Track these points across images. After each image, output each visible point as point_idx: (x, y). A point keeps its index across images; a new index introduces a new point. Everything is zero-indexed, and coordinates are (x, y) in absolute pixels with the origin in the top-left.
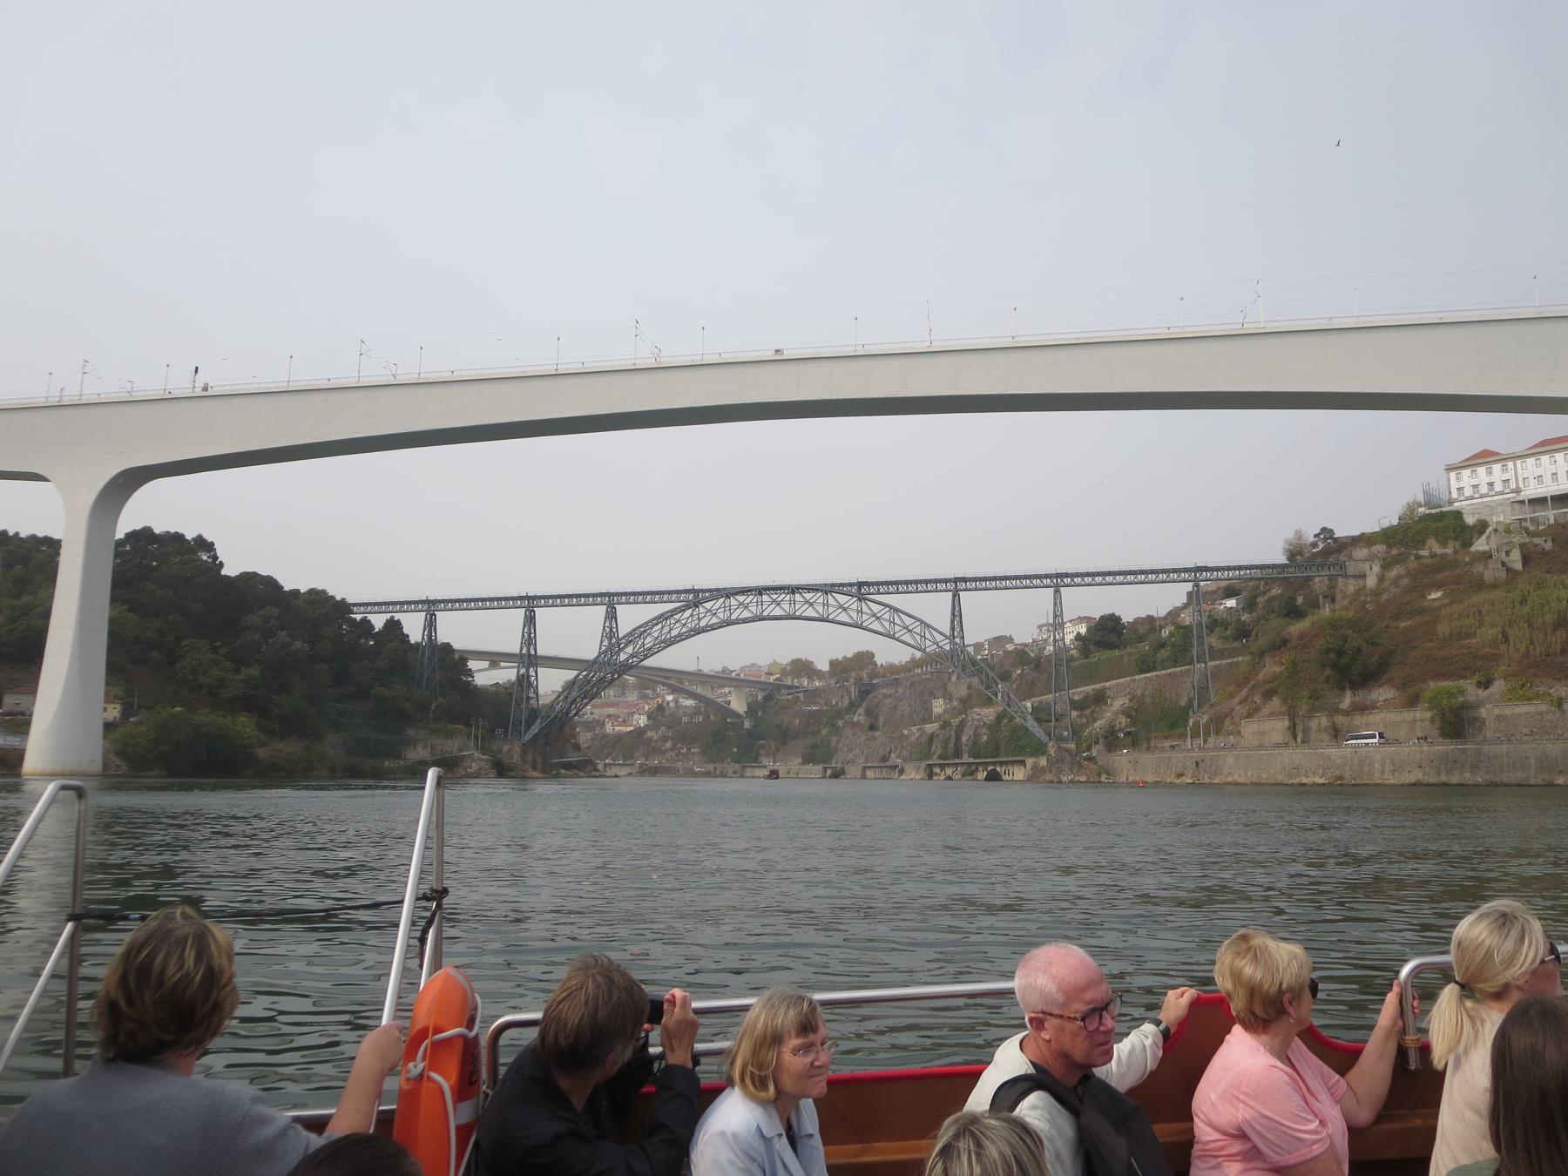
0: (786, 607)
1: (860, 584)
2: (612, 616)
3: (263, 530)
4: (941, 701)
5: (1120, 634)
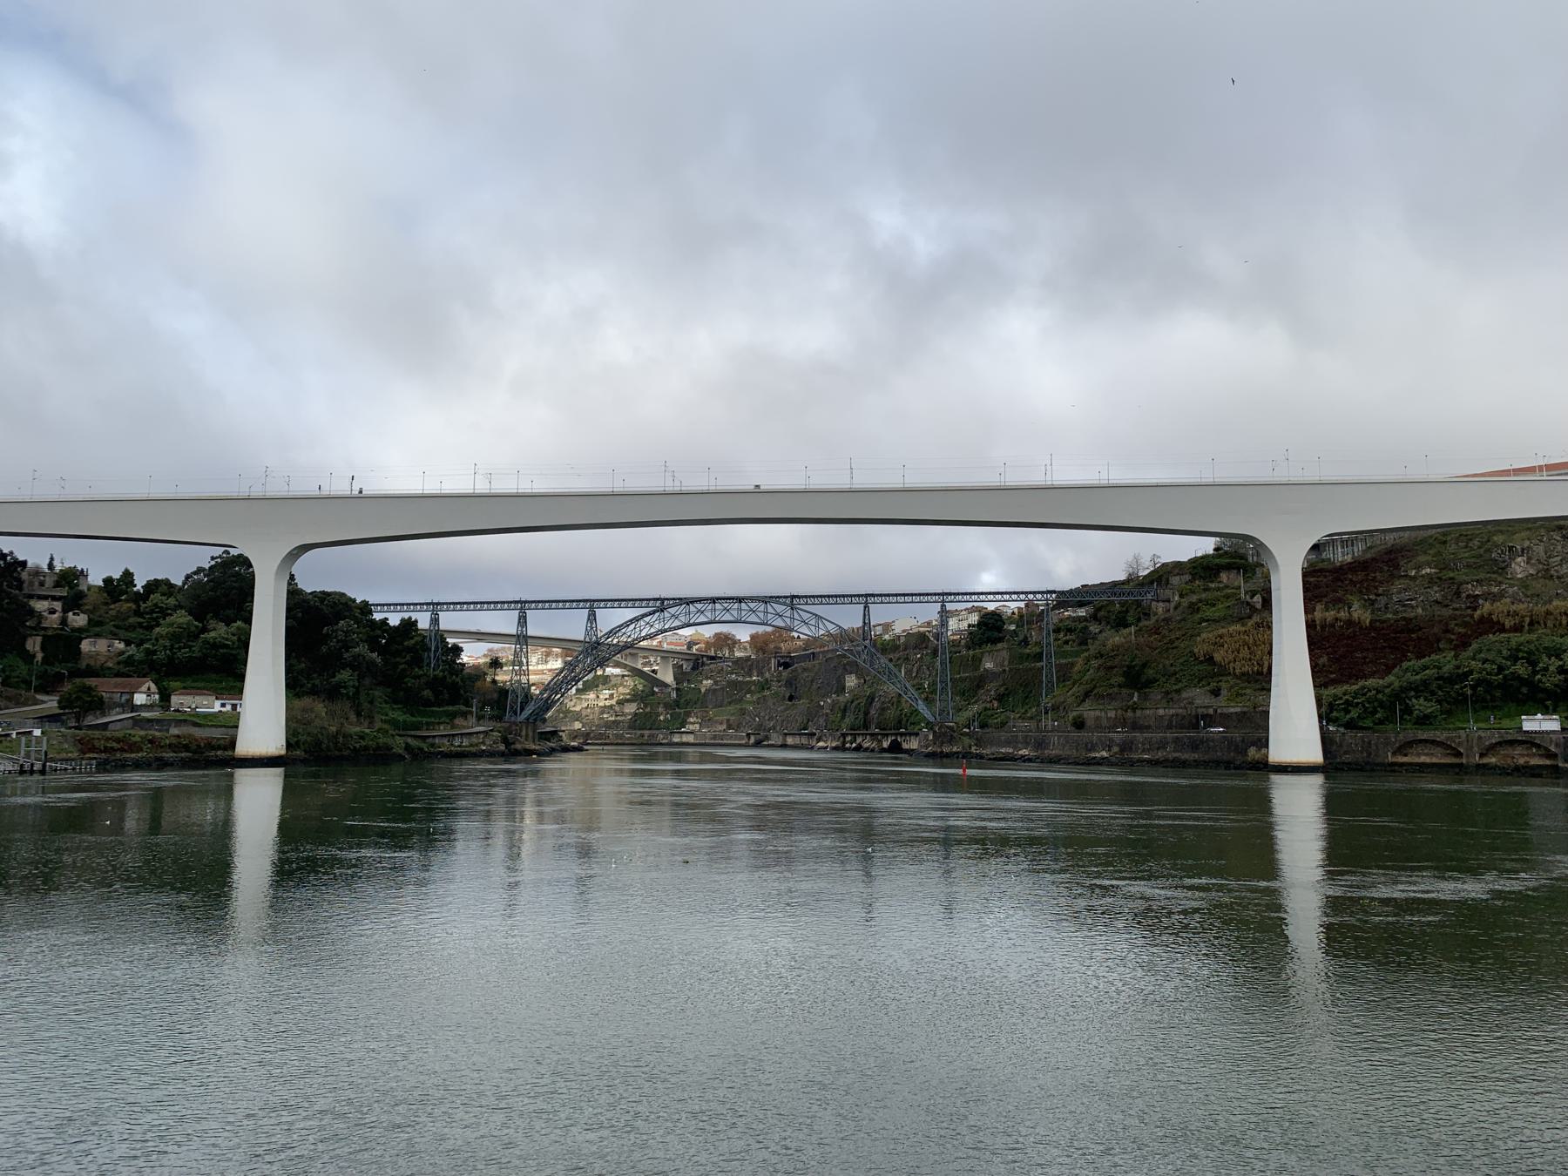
0: (735, 613)
1: (793, 597)
2: (592, 618)
3: (386, 582)
4: (853, 677)
5: (1000, 629)
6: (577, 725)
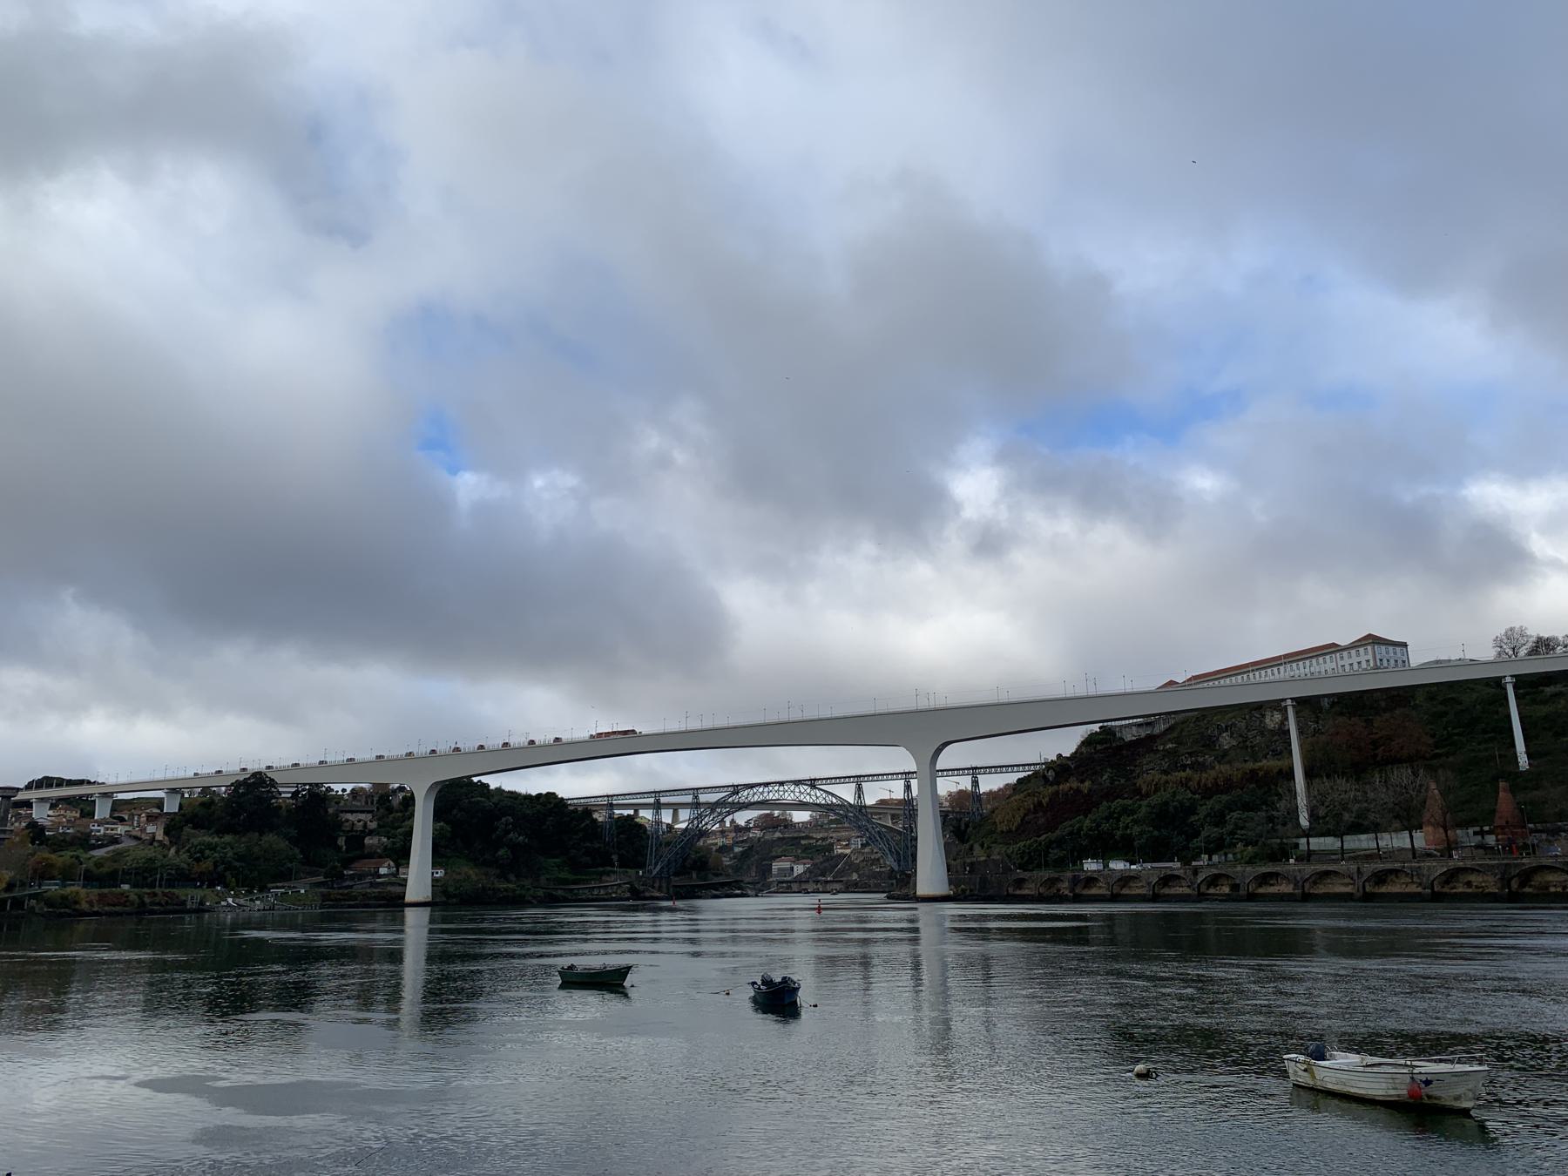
6: (855, 876)
